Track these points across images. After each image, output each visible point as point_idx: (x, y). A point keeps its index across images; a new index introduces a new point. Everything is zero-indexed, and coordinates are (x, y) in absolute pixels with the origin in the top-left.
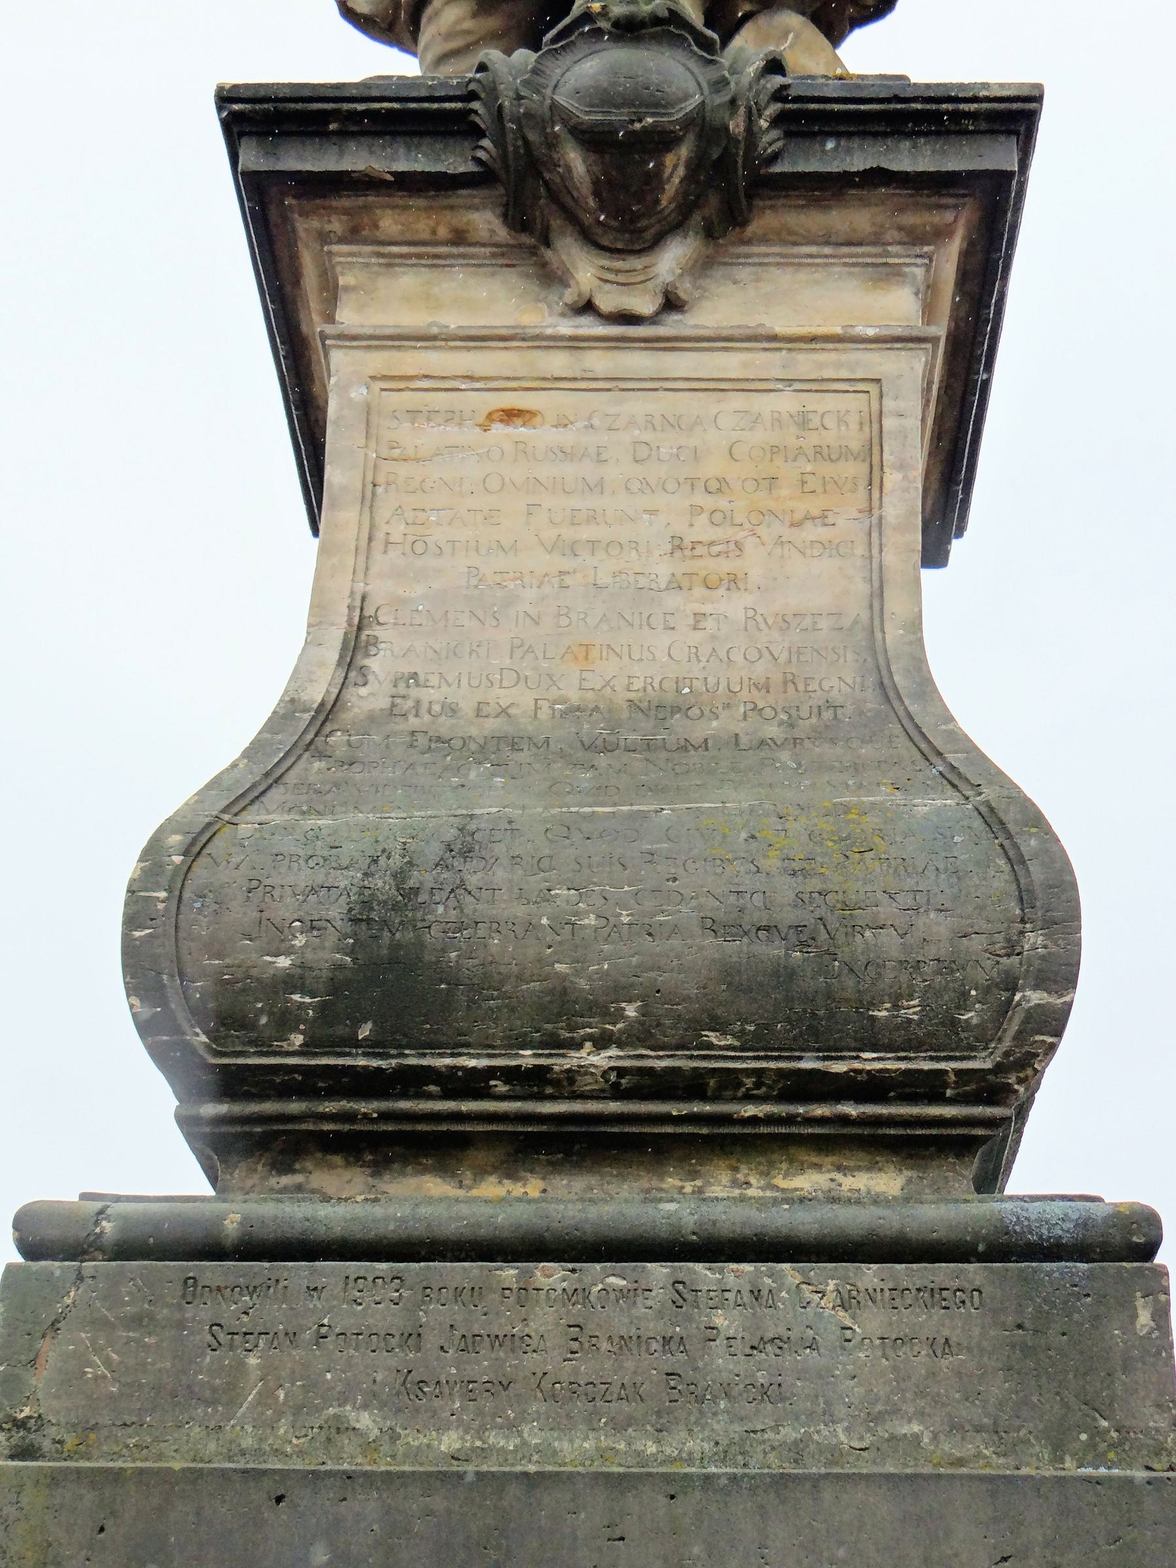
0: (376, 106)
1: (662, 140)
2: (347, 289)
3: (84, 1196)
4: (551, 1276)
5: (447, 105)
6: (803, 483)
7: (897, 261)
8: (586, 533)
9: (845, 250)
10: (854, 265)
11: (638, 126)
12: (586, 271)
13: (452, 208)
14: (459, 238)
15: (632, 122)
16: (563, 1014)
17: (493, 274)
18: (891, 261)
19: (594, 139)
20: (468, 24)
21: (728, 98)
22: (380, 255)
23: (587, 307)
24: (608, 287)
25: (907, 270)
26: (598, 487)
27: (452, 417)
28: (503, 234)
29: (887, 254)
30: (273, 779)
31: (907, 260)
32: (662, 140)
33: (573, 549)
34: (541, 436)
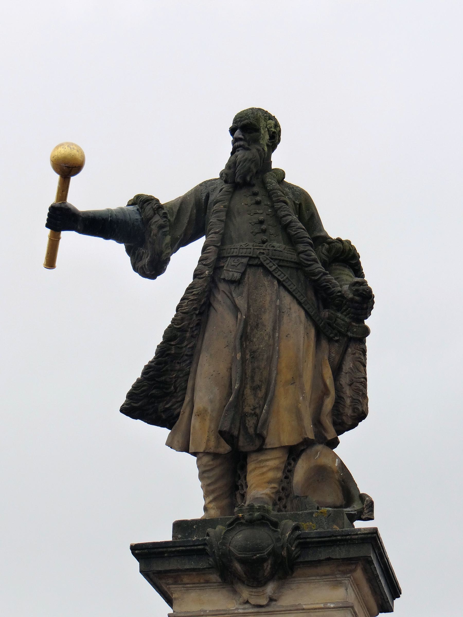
0: (178, 549)
1: (263, 560)
2: (175, 599)
5: (199, 547)
7: (340, 579)
9: (324, 577)
10: (327, 581)
11: (255, 557)
12: (245, 593)
13: (204, 574)
14: (207, 582)
15: (253, 556)
17: (219, 591)
18: (338, 579)
19: (242, 561)
20: (211, 463)
21: (281, 545)
22: (184, 587)
23: (247, 602)
24: (252, 597)
25: (343, 581)
28: (220, 580)
29: (336, 577)
31: (343, 579)
32: (263, 560)
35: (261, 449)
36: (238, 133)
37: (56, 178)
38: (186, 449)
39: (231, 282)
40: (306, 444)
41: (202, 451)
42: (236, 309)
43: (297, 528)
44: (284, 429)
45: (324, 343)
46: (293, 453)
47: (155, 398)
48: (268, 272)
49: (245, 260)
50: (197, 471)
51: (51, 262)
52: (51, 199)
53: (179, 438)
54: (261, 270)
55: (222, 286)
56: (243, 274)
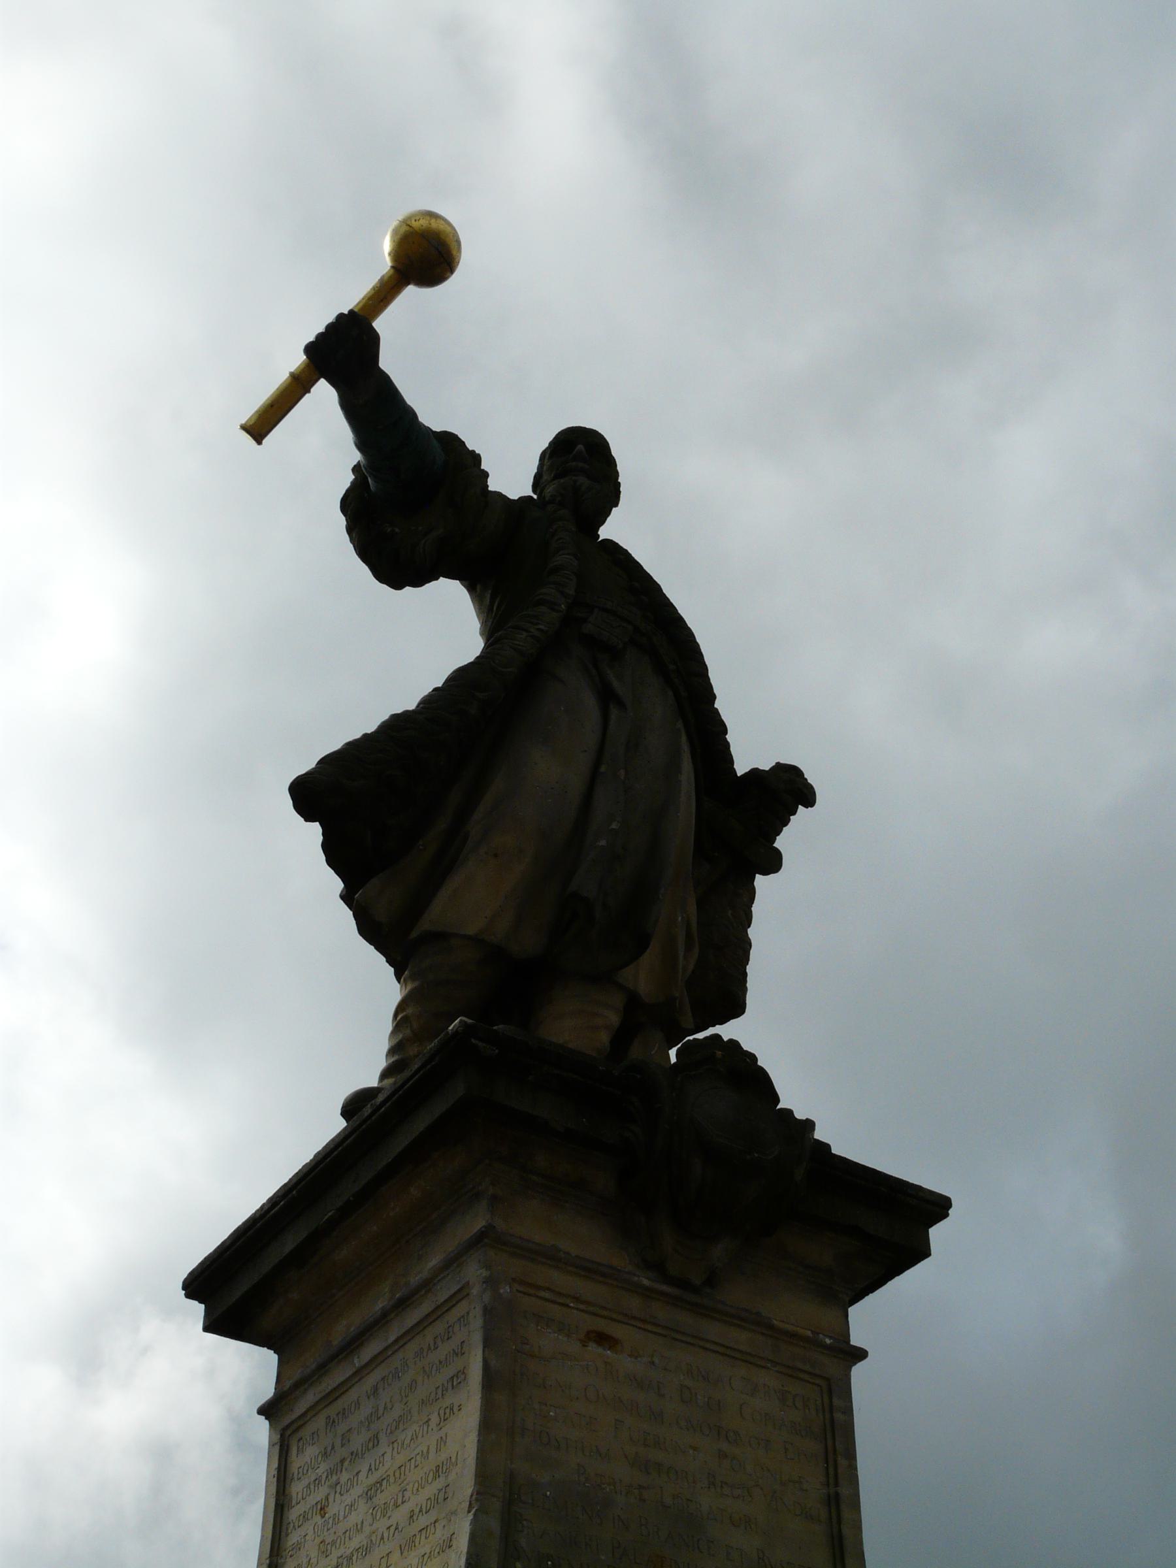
6: (786, 1450)
37: (384, 264)
41: (471, 930)
42: (607, 697)
51: (259, 428)
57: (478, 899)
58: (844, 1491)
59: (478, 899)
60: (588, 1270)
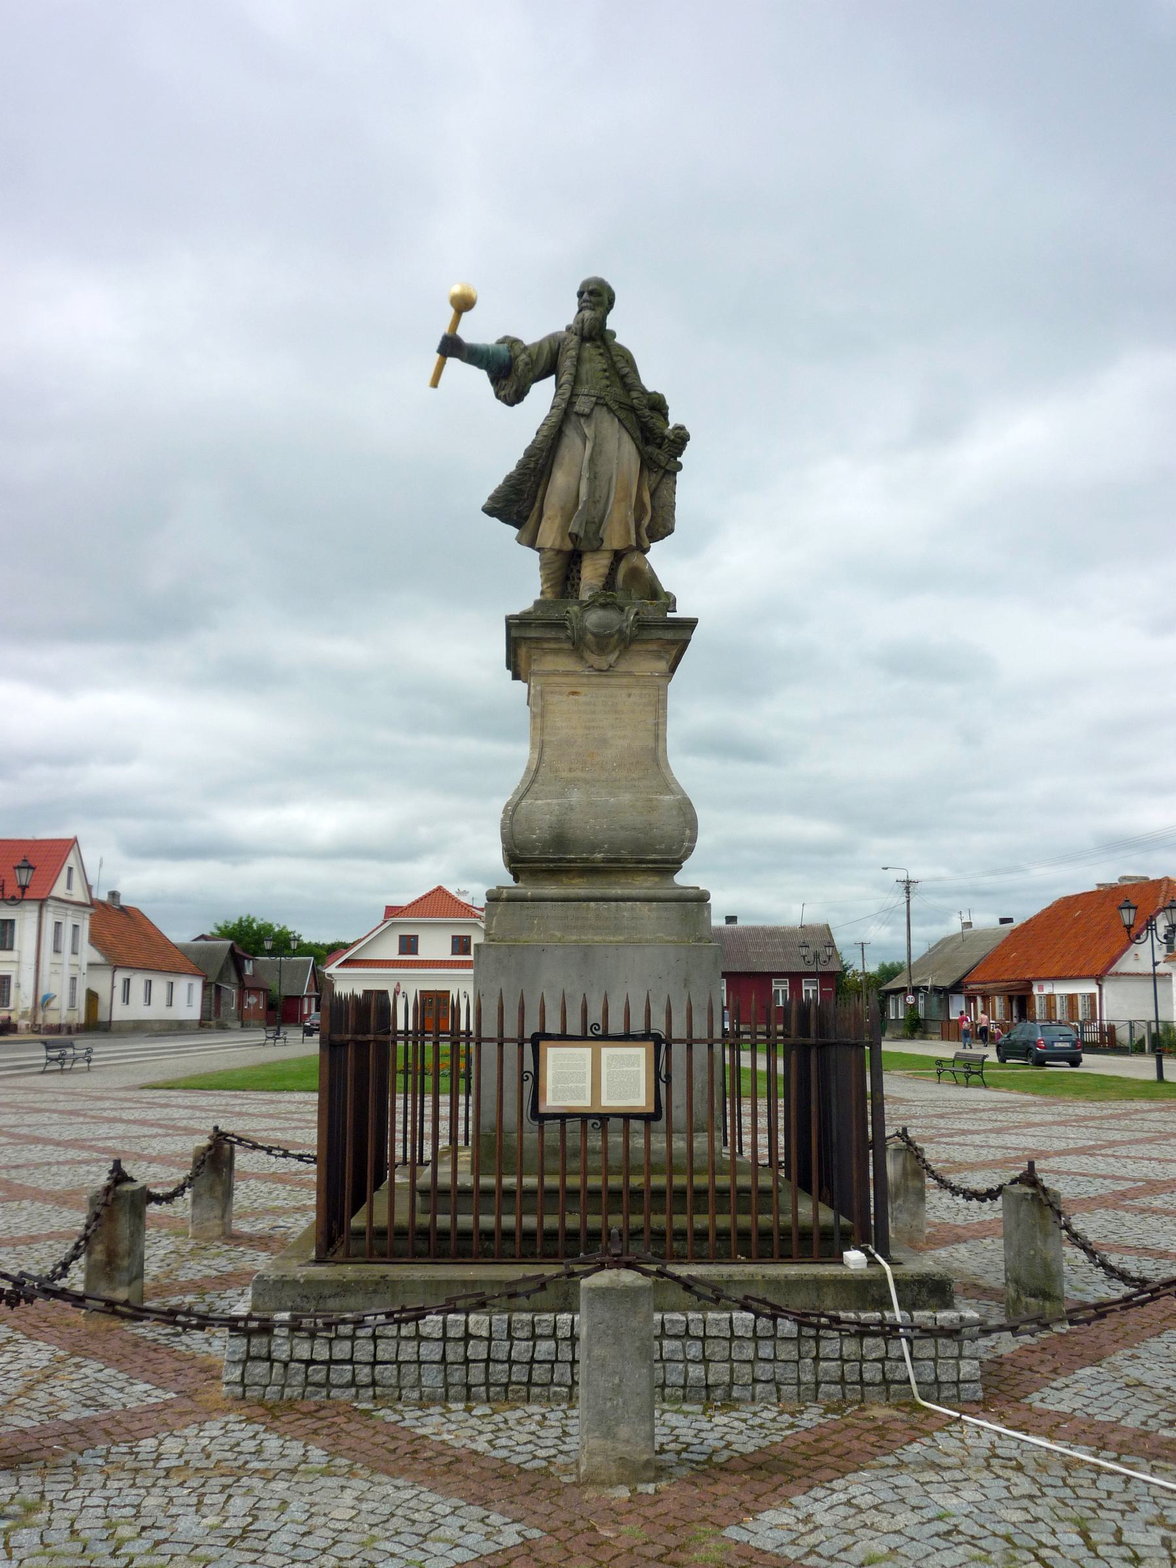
1: (611, 636)
3: (498, 888)
4: (592, 904)
8: (593, 724)
12: (593, 659)
16: (594, 848)
26: (594, 712)
27: (561, 694)
30: (528, 790)
33: (588, 728)
34: (581, 698)
35: (597, 550)
36: (585, 296)
37: (451, 312)
38: (532, 544)
39: (583, 415)
40: (630, 549)
41: (548, 546)
43: (637, 614)
44: (614, 538)
45: (646, 473)
46: (618, 556)
47: (516, 502)
48: (610, 410)
49: (594, 399)
50: (539, 564)
51: (435, 383)
52: (444, 329)
53: (527, 536)
54: (605, 408)
55: (574, 418)
56: (592, 410)
57: (550, 534)
58: (661, 720)
59: (550, 534)
60: (567, 674)
